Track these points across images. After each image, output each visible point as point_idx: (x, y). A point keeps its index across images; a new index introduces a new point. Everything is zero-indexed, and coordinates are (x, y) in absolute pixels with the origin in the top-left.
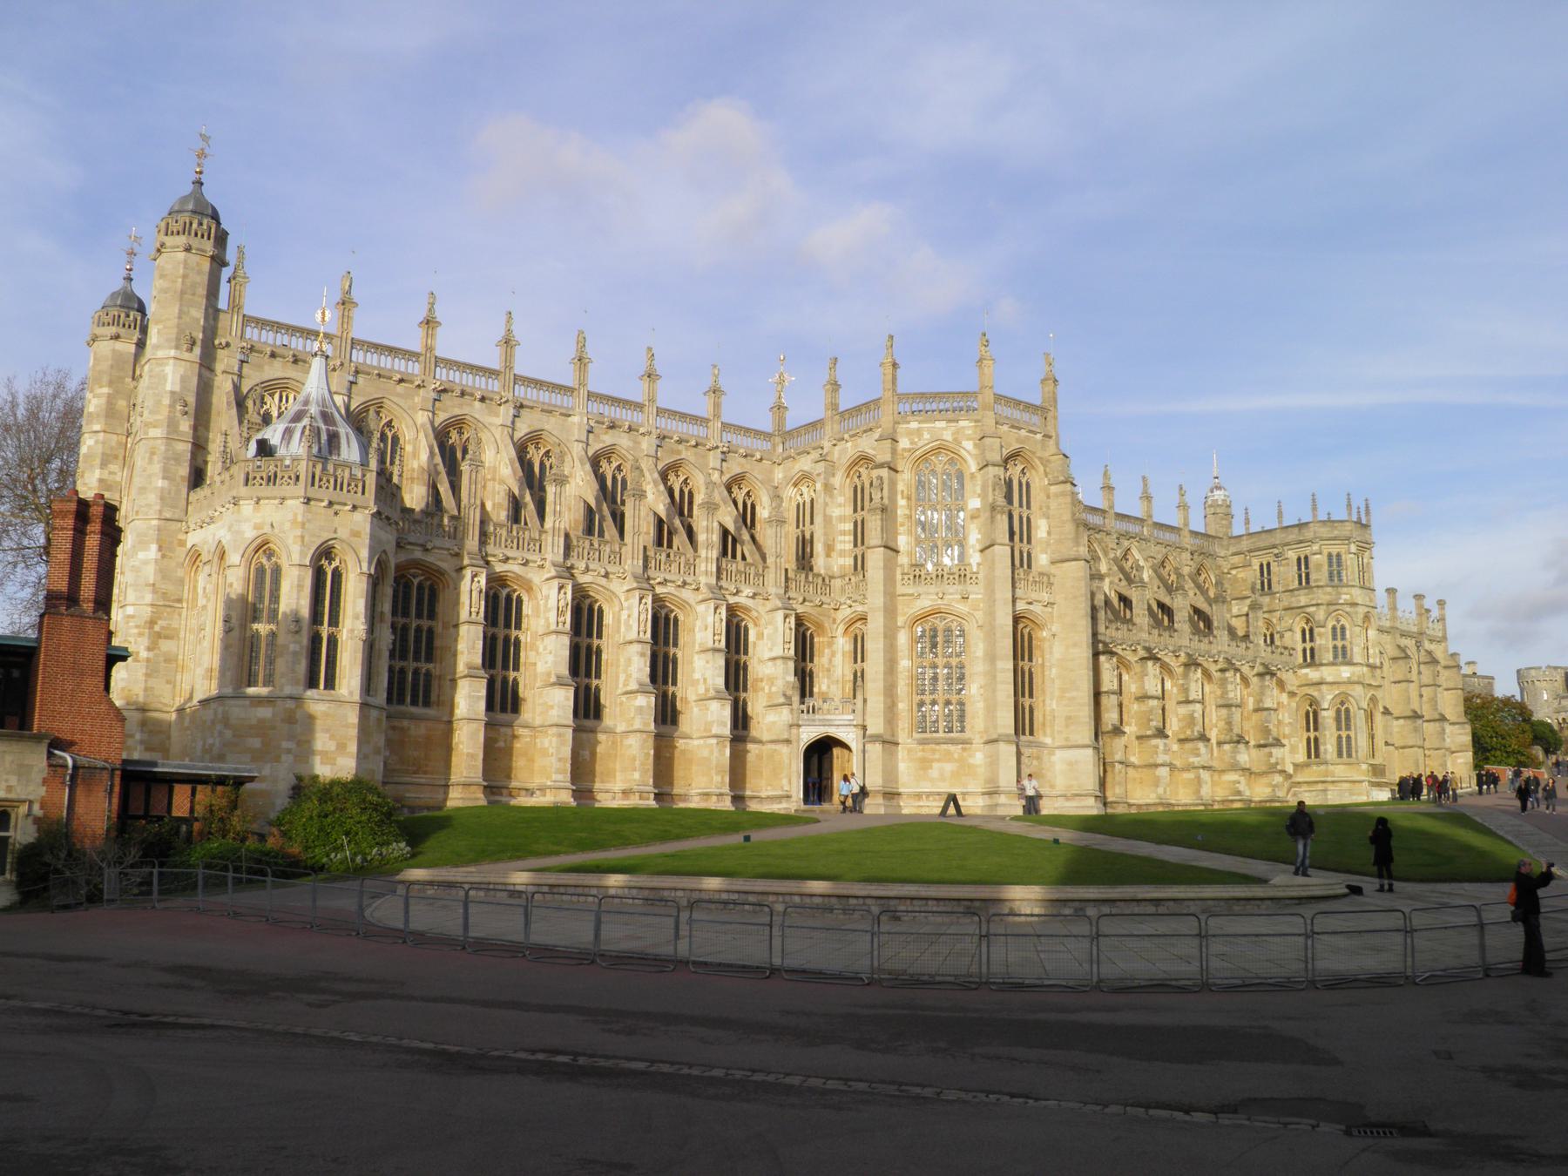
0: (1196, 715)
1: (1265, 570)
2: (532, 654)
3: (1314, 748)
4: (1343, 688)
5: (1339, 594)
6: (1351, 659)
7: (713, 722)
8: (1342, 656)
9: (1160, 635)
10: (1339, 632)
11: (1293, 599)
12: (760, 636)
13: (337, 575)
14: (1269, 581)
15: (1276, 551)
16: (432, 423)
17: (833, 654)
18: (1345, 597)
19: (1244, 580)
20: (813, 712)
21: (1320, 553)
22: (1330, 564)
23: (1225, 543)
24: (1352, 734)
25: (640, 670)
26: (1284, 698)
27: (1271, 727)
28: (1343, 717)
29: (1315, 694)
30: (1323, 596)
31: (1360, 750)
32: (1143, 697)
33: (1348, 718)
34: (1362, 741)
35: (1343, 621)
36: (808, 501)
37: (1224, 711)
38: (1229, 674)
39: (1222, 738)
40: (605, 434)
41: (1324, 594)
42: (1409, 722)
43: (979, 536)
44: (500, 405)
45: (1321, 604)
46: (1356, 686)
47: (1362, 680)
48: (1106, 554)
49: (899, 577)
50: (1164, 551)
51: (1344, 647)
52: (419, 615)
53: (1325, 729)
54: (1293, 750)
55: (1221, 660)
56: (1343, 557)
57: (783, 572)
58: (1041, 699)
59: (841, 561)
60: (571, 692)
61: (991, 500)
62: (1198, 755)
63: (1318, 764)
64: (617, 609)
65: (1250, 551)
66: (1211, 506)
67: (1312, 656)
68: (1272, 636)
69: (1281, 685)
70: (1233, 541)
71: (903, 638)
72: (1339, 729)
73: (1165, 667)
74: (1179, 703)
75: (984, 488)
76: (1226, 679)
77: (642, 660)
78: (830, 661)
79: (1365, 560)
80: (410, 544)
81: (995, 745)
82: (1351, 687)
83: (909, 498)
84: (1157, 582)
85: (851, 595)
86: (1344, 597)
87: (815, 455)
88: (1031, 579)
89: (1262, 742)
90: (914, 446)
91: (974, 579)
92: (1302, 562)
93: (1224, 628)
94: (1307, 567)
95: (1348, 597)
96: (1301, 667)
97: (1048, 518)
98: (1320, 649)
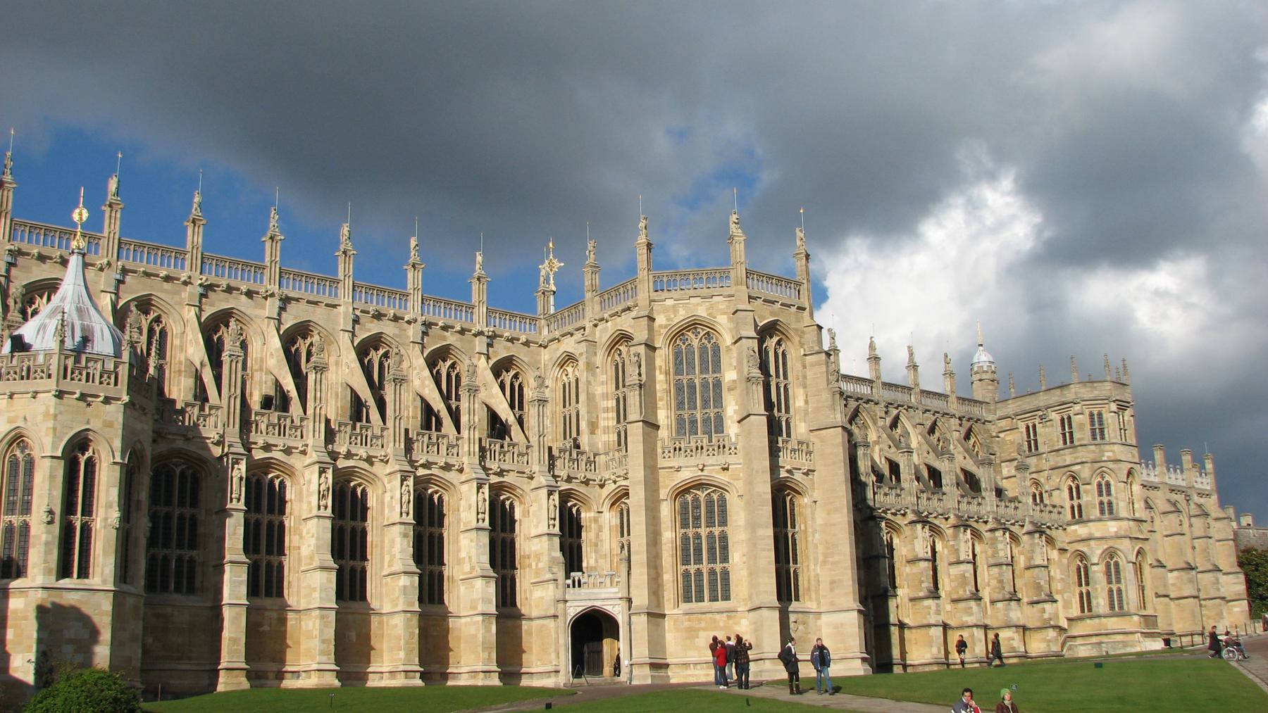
0: (967, 575)
1: (1031, 432)
2: (295, 539)
3: (1086, 601)
4: (1111, 543)
5: (1102, 452)
6: (1117, 513)
7: (479, 599)
8: (1108, 510)
9: (928, 499)
10: (1105, 488)
12: (526, 513)
13: (90, 464)
14: (1036, 441)
15: (1040, 413)
16: (199, 318)
17: (600, 529)
19: (1012, 443)
20: (579, 586)
21: (1082, 414)
22: (1092, 423)
23: (992, 407)
25: (402, 551)
26: (1054, 554)
27: (1042, 583)
29: (1085, 549)
30: (1082, 454)
31: (1130, 602)
32: (914, 561)
33: (1118, 572)
34: (1131, 595)
35: (1107, 478)
36: (573, 381)
37: (996, 570)
38: (999, 534)
39: (996, 596)
40: (372, 322)
41: (1088, 452)
42: (1182, 573)
43: (737, 408)
44: (266, 298)
46: (1124, 540)
48: (875, 423)
49: (659, 451)
50: (933, 418)
51: (1110, 503)
52: (182, 504)
53: (1095, 583)
54: (1067, 605)
55: (990, 520)
56: (1104, 416)
57: (546, 450)
58: (805, 564)
59: (605, 438)
60: (333, 575)
61: (746, 373)
62: (971, 614)
63: (1091, 618)
64: (380, 492)
66: (977, 373)
67: (1080, 516)
68: (1041, 495)
69: (1050, 541)
70: (999, 405)
71: (666, 510)
72: (1110, 582)
73: (935, 530)
74: (951, 564)
75: (740, 362)
76: (996, 538)
77: (405, 540)
78: (597, 536)
79: (1126, 418)
80: (170, 434)
81: (759, 612)
82: (1119, 541)
83: (668, 373)
84: (926, 447)
85: (615, 470)
86: (1107, 454)
87: (578, 336)
88: (790, 448)
89: (1035, 599)
90: (671, 322)
91: (733, 450)
92: (1066, 423)
93: (991, 490)
95: (1110, 454)
96: (1069, 525)
97: (805, 387)
98: (1087, 506)
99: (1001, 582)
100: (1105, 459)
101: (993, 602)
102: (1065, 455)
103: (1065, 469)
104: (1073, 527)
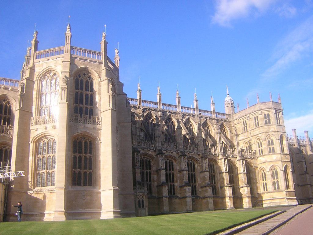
0: (206, 176)
1: (245, 123)
5: (269, 128)
8: (272, 151)
11: (254, 133)
15: (247, 116)
18: (271, 130)
21: (262, 114)
22: (265, 118)
24: (279, 181)
31: (282, 186)
45: (263, 133)
51: (273, 148)
55: (220, 155)
56: (270, 115)
63: (267, 193)
65: (239, 118)
67: (262, 154)
82: (277, 162)
86: (271, 129)
92: (256, 118)
100: (271, 131)
102: (255, 131)
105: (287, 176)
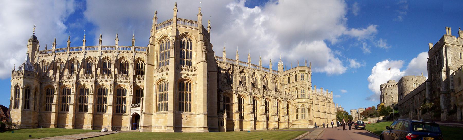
0: (263, 109)
1: (289, 78)
4: (303, 103)
5: (303, 83)
8: (303, 96)
10: (303, 91)
11: (294, 84)
15: (291, 74)
23: (281, 73)
28: (303, 110)
29: (297, 105)
30: (299, 83)
32: (248, 105)
33: (304, 110)
35: (304, 89)
37: (273, 108)
39: (273, 115)
47: (307, 102)
51: (304, 94)
55: (273, 96)
56: (304, 74)
66: (279, 65)
68: (290, 93)
74: (260, 106)
82: (305, 103)
86: (304, 83)
89: (284, 115)
92: (296, 76)
94: (297, 77)
96: (295, 99)
98: (299, 95)
99: (274, 111)
100: (303, 84)
101: (272, 116)
103: (295, 87)
104: (296, 100)
105: (310, 111)
